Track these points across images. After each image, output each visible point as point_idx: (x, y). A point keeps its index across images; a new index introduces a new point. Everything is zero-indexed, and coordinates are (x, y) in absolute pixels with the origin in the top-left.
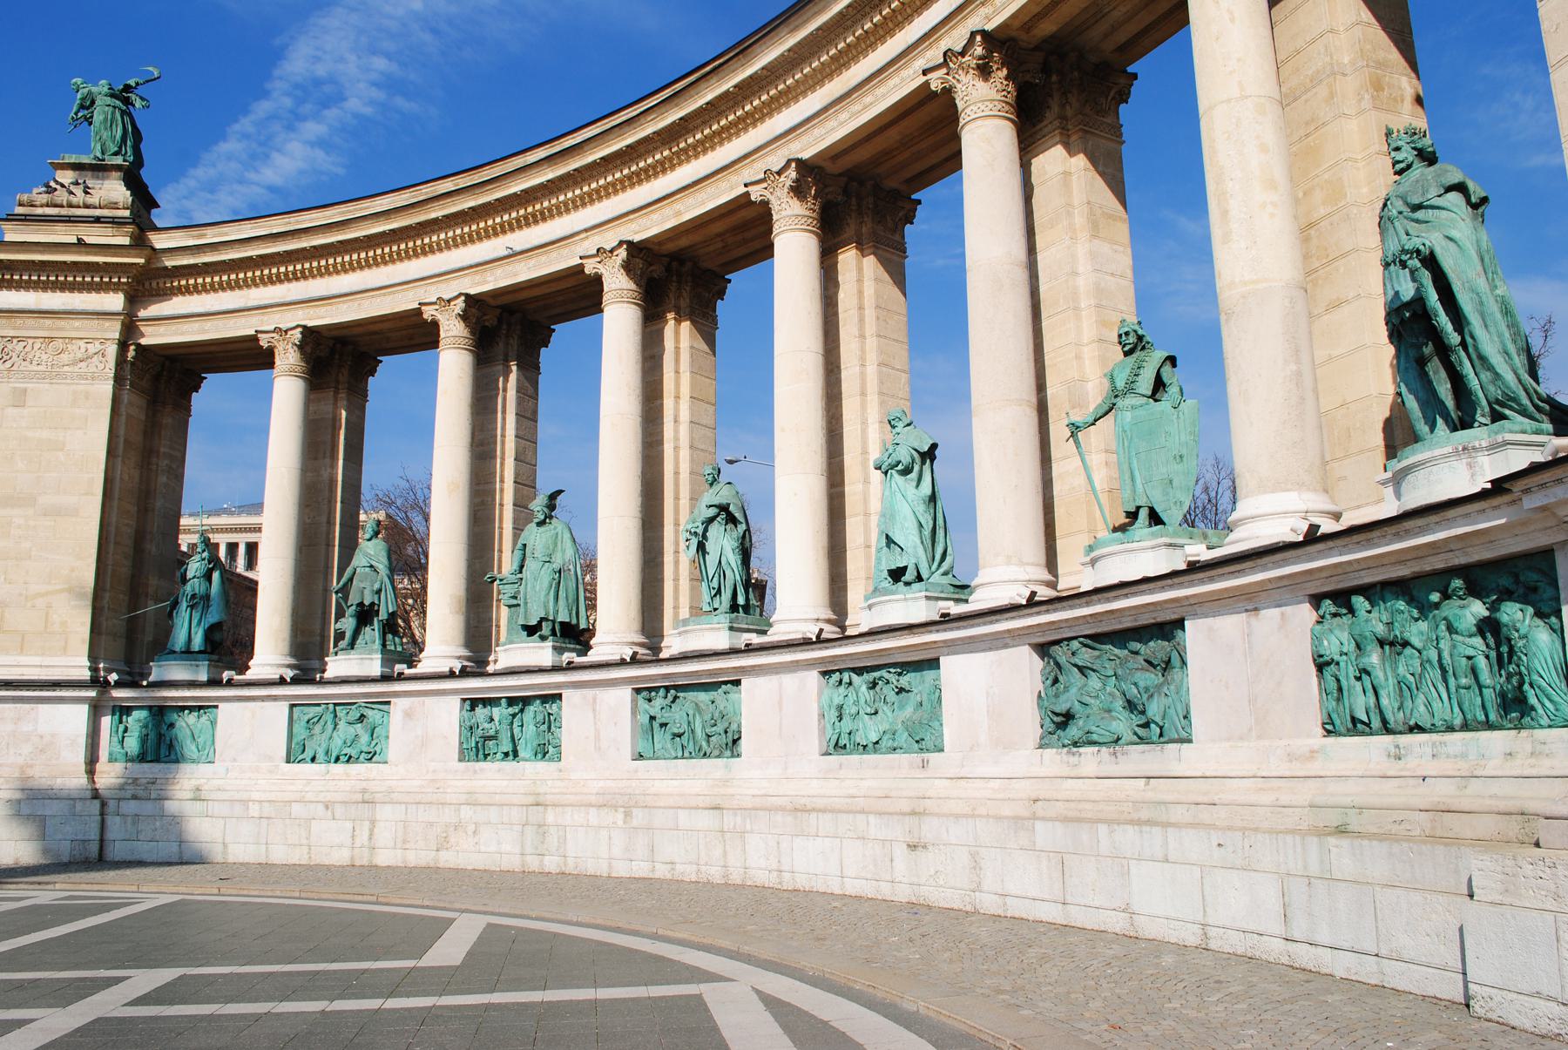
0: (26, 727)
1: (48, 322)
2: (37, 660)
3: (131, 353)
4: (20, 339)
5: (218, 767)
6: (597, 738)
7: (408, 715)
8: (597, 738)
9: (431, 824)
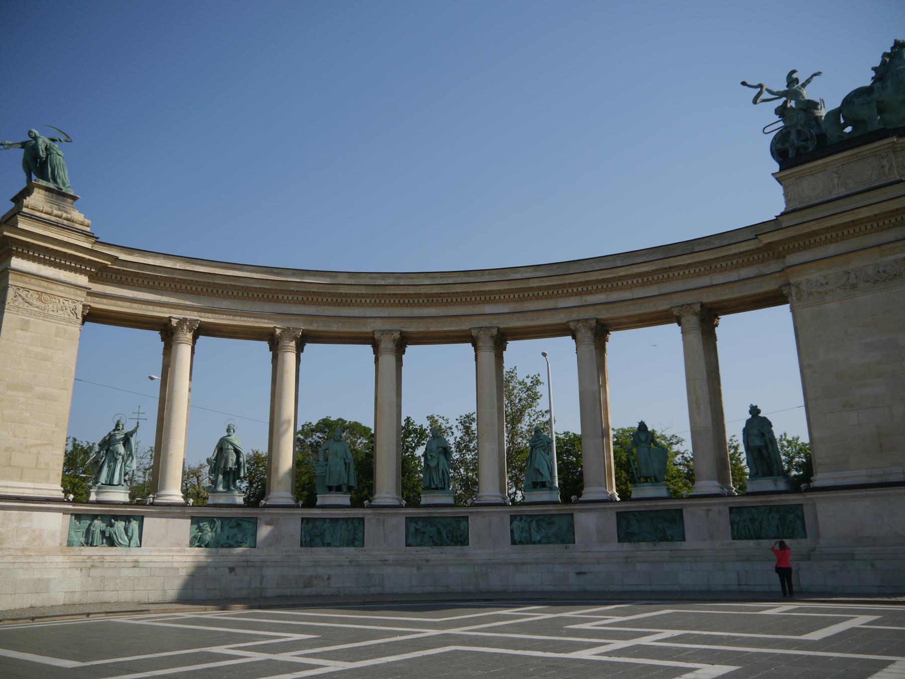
4: (28, 290)
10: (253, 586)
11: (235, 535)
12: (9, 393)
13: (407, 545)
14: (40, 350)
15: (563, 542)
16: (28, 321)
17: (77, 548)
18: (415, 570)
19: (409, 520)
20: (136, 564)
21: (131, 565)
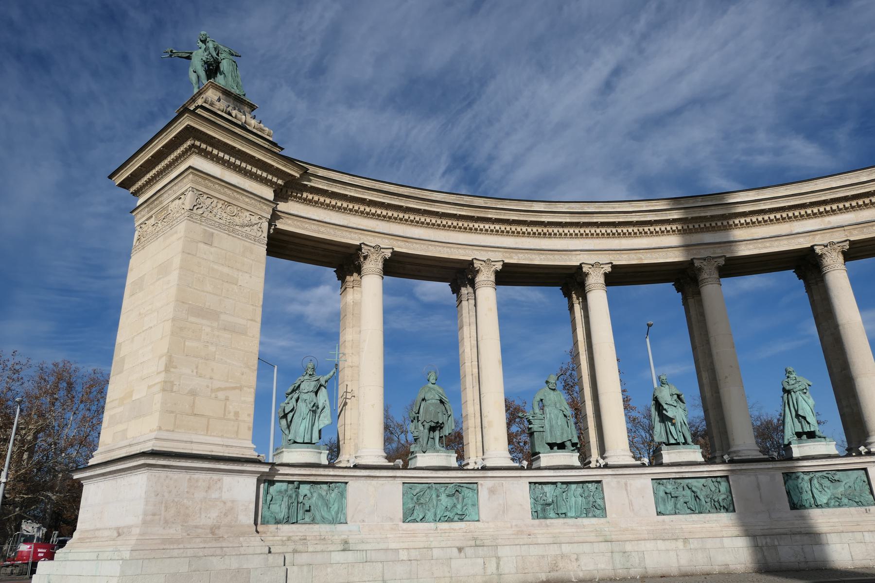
0: (214, 495)
1: (229, 192)
2: (218, 440)
3: (272, 231)
4: (210, 197)
5: (351, 526)
6: (631, 504)
7: (492, 491)
8: (631, 504)
9: (543, 556)
10: (489, 572)
11: (455, 506)
12: (192, 319)
13: (659, 513)
14: (226, 270)
15: (859, 504)
16: (212, 234)
17: (272, 527)
18: (680, 544)
19: (658, 481)
20: (346, 547)
21: (341, 547)
